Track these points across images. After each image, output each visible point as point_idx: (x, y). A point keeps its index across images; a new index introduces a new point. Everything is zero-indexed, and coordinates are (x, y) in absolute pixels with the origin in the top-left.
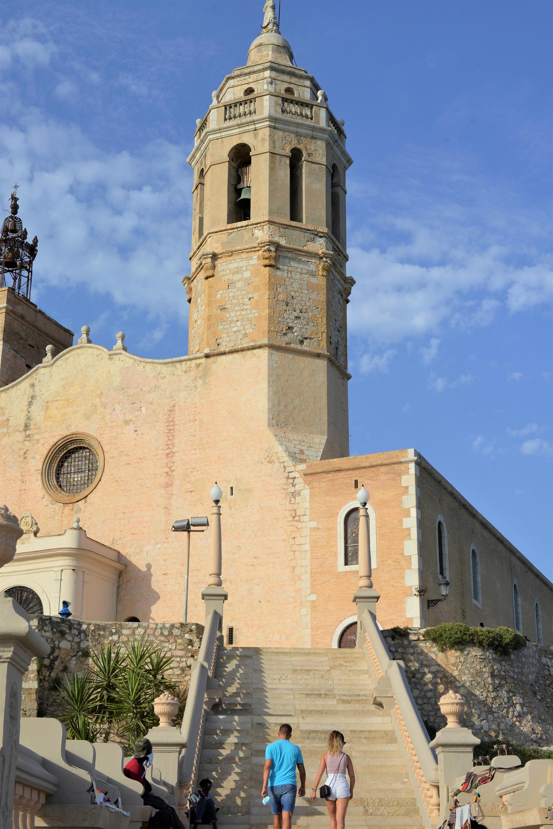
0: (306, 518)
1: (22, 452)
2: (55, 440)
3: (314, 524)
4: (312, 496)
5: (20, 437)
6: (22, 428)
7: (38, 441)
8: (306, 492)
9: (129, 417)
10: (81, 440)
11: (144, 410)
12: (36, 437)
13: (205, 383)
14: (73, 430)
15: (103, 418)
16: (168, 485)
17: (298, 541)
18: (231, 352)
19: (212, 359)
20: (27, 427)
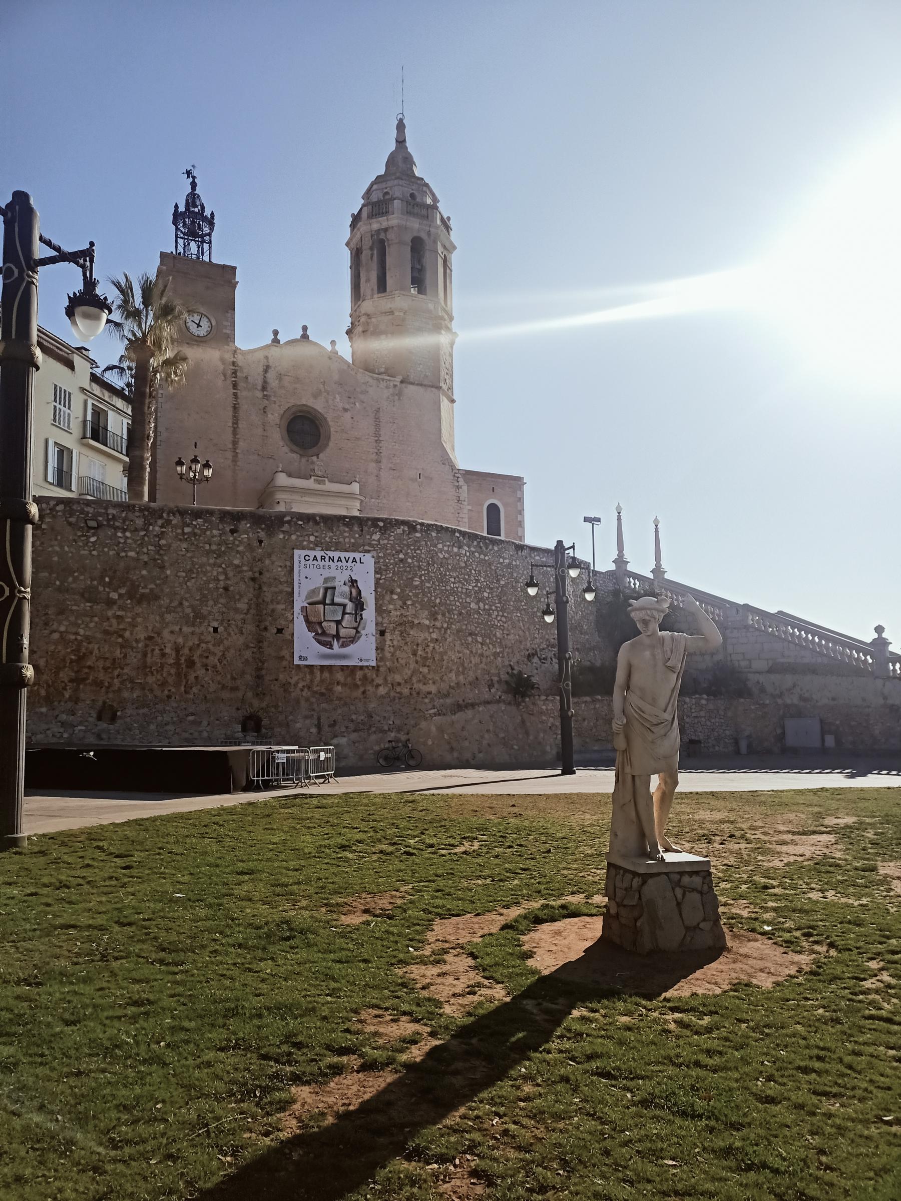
0: (466, 503)
1: (262, 407)
2: (289, 405)
3: (470, 507)
4: (468, 490)
5: (259, 394)
6: (260, 388)
7: (275, 402)
8: (465, 488)
9: (347, 406)
10: (308, 412)
11: (357, 404)
12: (273, 399)
13: (399, 399)
14: (304, 402)
15: (327, 401)
16: (378, 462)
17: (461, 515)
18: (418, 385)
19: (404, 385)
20: (264, 388)
